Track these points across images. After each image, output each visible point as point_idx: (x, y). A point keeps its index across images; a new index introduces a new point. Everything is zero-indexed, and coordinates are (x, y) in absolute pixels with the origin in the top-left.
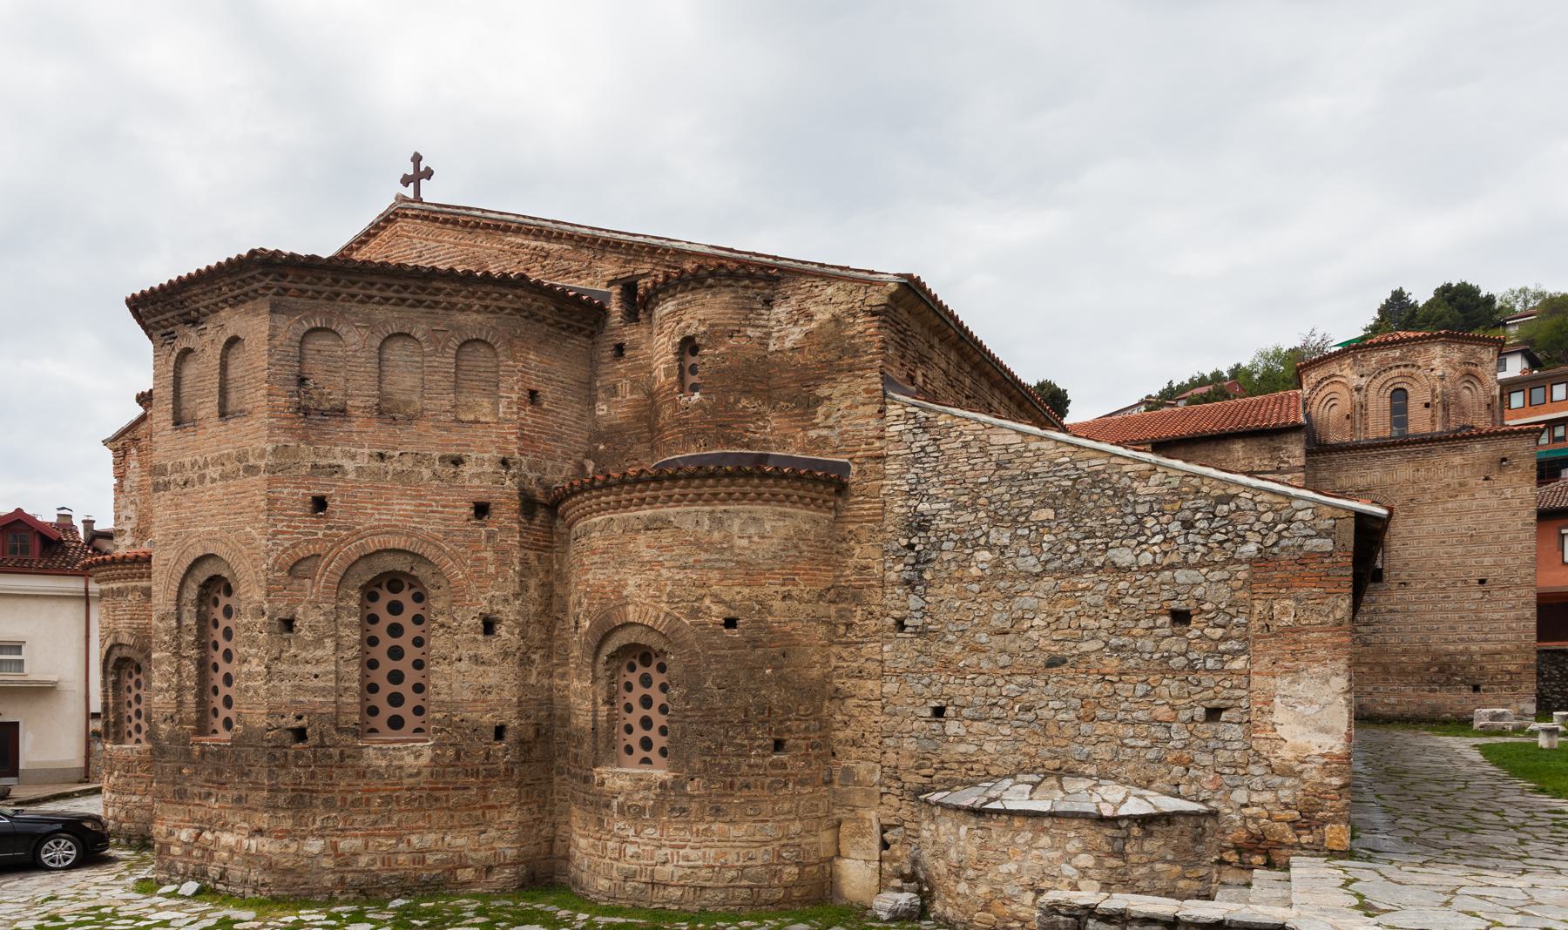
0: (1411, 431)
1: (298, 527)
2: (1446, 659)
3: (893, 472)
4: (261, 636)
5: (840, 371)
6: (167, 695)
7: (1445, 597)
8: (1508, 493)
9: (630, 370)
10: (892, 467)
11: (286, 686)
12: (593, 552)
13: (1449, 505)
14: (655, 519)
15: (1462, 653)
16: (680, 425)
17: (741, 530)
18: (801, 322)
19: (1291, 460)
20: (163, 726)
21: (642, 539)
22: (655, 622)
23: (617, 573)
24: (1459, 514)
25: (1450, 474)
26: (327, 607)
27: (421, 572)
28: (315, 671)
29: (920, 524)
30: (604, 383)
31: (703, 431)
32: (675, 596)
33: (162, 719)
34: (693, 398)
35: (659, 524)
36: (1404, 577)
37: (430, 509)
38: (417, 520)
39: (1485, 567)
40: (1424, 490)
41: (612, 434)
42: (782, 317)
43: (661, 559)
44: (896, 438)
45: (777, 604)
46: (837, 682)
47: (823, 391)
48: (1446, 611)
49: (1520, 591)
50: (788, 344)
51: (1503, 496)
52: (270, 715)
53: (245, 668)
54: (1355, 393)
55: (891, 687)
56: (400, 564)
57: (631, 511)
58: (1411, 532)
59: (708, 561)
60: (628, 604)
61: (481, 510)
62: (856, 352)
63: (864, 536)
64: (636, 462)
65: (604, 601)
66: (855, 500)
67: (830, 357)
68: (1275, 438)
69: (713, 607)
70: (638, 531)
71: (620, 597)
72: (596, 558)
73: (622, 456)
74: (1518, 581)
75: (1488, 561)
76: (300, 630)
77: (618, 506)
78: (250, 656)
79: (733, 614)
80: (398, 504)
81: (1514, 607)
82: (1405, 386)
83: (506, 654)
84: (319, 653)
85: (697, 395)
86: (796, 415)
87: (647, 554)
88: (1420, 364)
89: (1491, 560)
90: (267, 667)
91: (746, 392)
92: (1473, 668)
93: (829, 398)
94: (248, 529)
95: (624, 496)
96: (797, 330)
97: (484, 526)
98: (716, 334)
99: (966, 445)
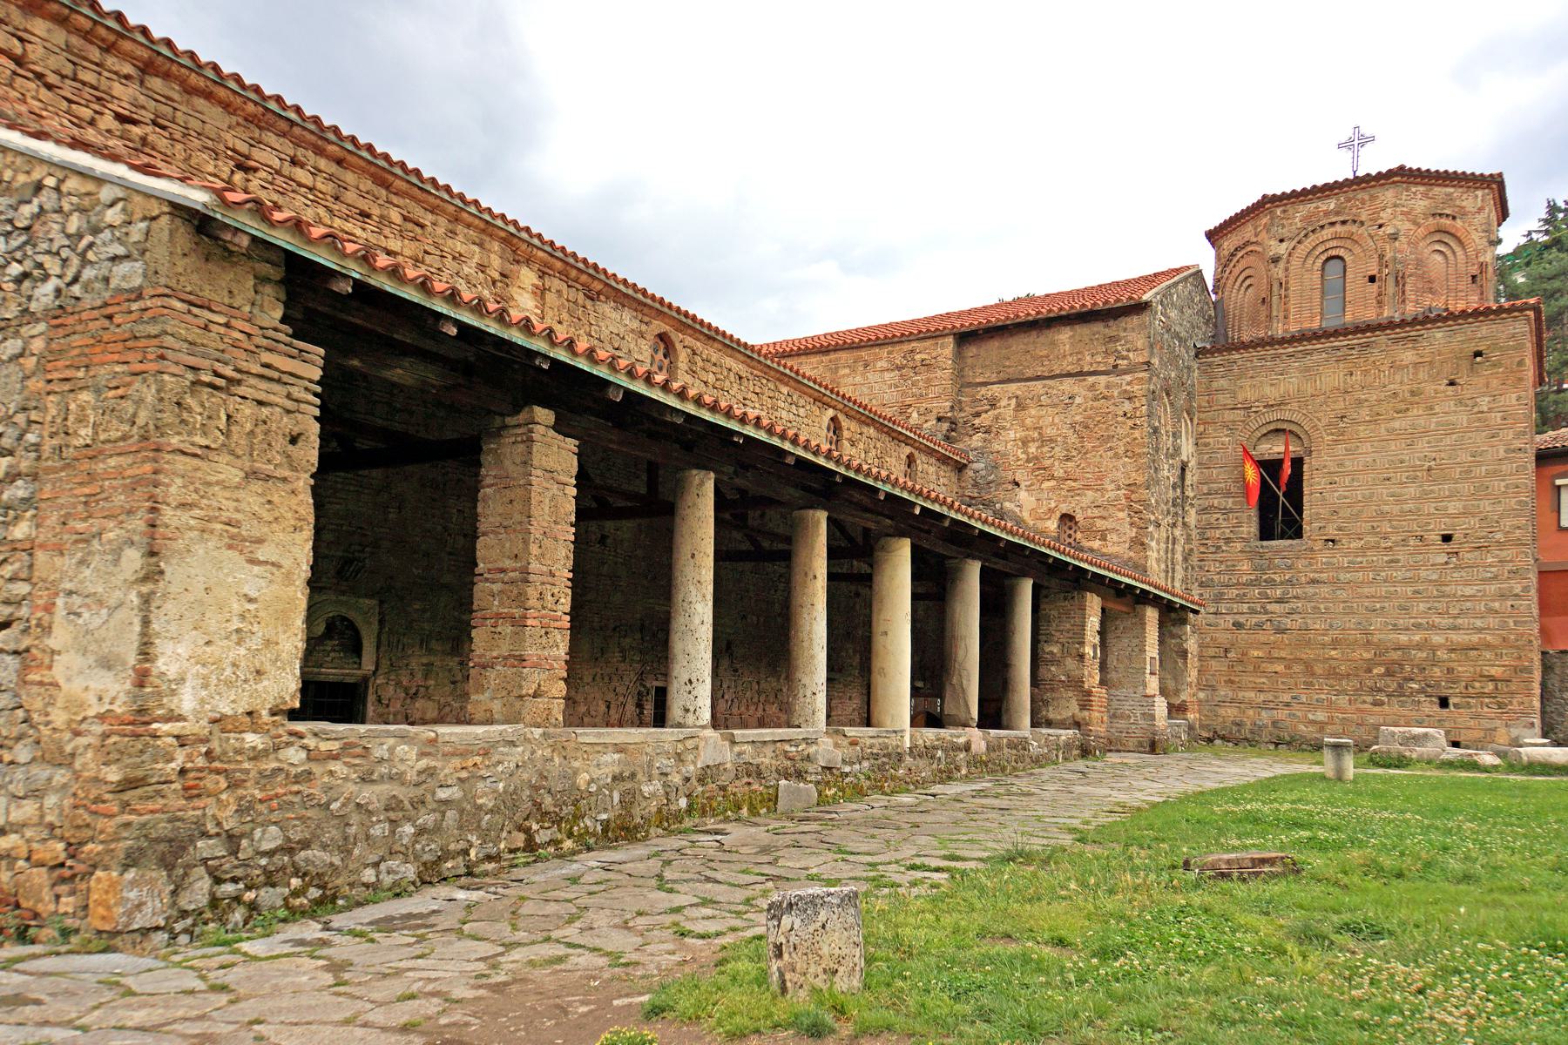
0: (1348, 318)
2: (1396, 655)
7: (1392, 561)
8: (1484, 403)
13: (1396, 424)
15: (1419, 647)
19: (1131, 355)
24: (1412, 436)
25: (1398, 378)
36: (1331, 531)
39: (1448, 516)
40: (1360, 402)
48: (1394, 582)
49: (1504, 554)
51: (1476, 410)
54: (1272, 265)
58: (1341, 465)
68: (1111, 323)
74: (1499, 536)
75: (1454, 507)
81: (1495, 577)
82: (1341, 252)
88: (1363, 218)
89: (1459, 505)
92: (1436, 669)
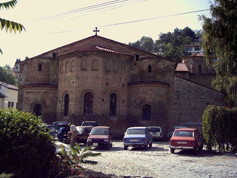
10: (175, 84)
14: (151, 89)
21: (149, 91)
27: (117, 94)
29: (179, 91)
45: (164, 100)
46: (167, 111)
47: (166, 74)
50: (161, 67)
55: (175, 111)
56: (114, 92)
61: (123, 85)
62: (170, 70)
67: (167, 70)
77: (146, 87)
83: (125, 105)
87: (150, 93)
98: (154, 66)
99: (184, 83)
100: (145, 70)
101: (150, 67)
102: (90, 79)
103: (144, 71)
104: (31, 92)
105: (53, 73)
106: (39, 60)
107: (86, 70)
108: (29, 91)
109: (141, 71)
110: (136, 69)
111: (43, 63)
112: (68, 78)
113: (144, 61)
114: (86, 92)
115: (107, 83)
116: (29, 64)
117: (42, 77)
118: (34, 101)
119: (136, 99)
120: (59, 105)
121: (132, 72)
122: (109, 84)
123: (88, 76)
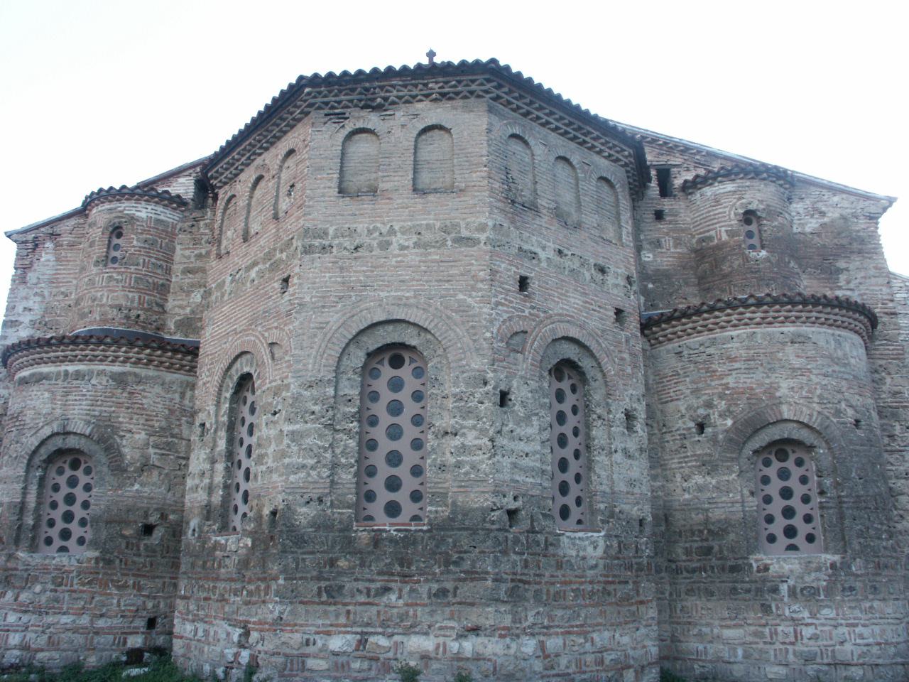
1: (511, 302)
3: (904, 325)
4: (482, 407)
5: (852, 252)
6: (313, 473)
9: (671, 230)
11: (506, 462)
12: (732, 360)
16: (752, 272)
17: (851, 352)
18: (816, 216)
20: (304, 510)
21: (790, 349)
22: (810, 419)
23: (768, 377)
26: (533, 384)
27: (586, 364)
28: (527, 449)
30: (648, 237)
31: (773, 279)
32: (824, 398)
33: (303, 501)
34: (761, 254)
35: (803, 340)
37: (592, 307)
38: (585, 315)
41: (660, 276)
42: (801, 211)
43: (809, 367)
44: (903, 302)
47: (841, 264)
50: (808, 230)
52: (496, 493)
53: (457, 441)
56: (571, 352)
57: (775, 327)
59: (840, 372)
60: (781, 403)
63: (893, 369)
64: (684, 301)
65: (753, 401)
66: (880, 343)
69: (848, 410)
70: (784, 344)
71: (772, 396)
72: (736, 365)
73: (671, 295)
76: (514, 405)
78: (465, 427)
79: (859, 416)
80: (573, 297)
84: (529, 431)
85: (764, 253)
86: (823, 278)
87: (797, 363)
90: (492, 440)
91: (792, 256)
93: (847, 270)
94: (461, 296)
95: (771, 314)
96: (814, 221)
97: (622, 330)
100: (725, 237)
101: (749, 216)
102: (402, 248)
103: (719, 247)
104: (39, 378)
105: (189, 279)
106: (112, 206)
107: (373, 191)
108: (32, 375)
109: (696, 251)
110: (668, 242)
111: (132, 219)
112: (255, 264)
113: (708, 191)
114: (373, 342)
115: (523, 283)
116: (65, 239)
117: (120, 297)
118: (47, 431)
119: (709, 405)
120: (198, 461)
121: (648, 257)
122: (534, 285)
123: (392, 232)
